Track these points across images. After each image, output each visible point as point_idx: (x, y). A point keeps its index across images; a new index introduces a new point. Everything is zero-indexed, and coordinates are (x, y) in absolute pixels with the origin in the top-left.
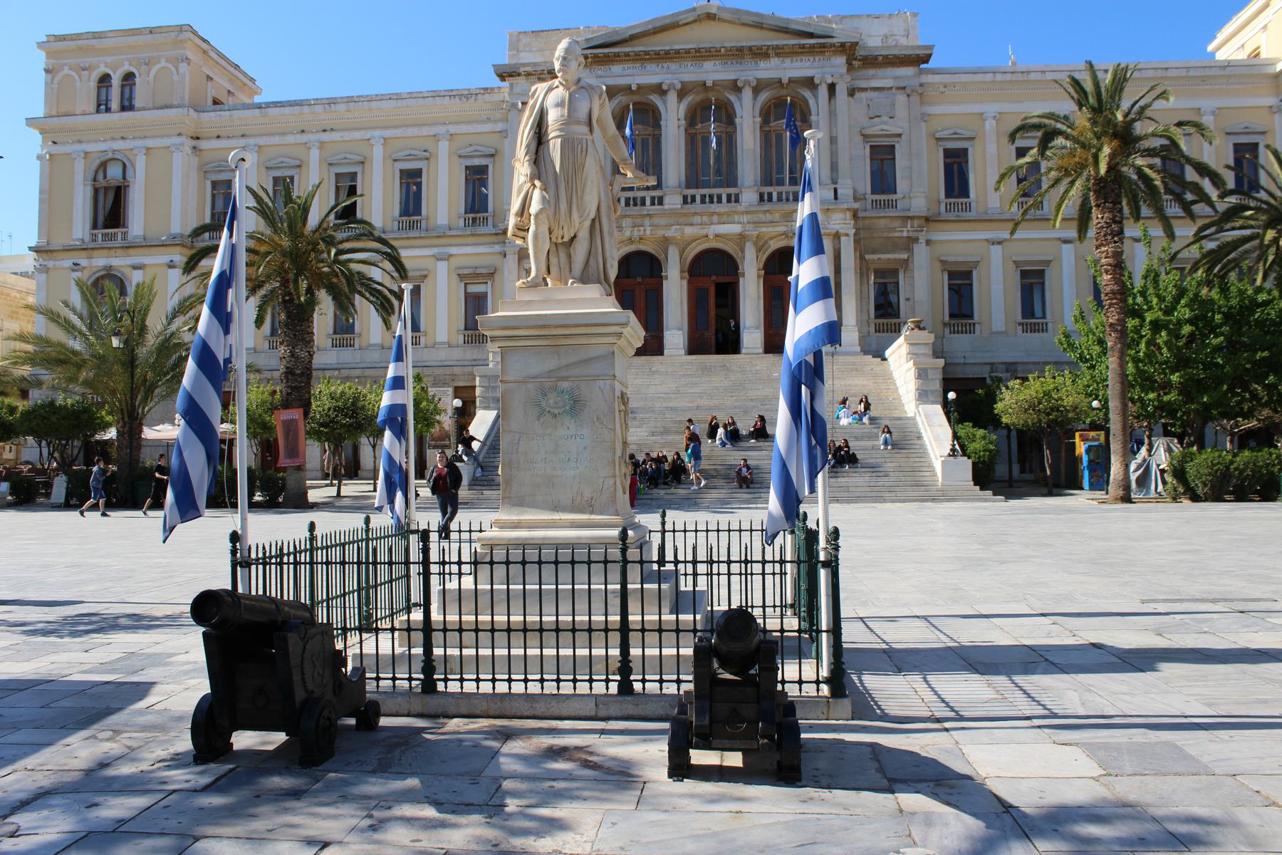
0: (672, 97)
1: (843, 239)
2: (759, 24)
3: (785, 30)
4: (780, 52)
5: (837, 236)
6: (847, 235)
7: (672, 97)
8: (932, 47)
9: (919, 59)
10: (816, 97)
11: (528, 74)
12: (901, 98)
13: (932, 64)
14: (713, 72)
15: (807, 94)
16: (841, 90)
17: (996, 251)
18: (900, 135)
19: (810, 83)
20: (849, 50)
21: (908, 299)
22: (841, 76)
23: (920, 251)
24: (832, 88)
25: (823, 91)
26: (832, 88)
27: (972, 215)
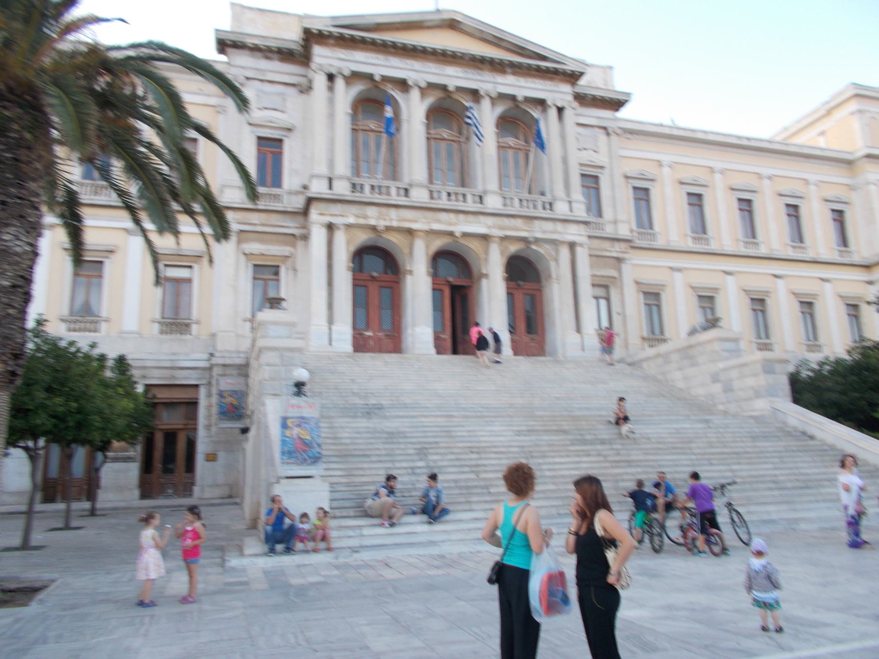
0: (415, 94)
1: (579, 250)
2: (497, 40)
3: (521, 50)
4: (517, 69)
5: (572, 246)
6: (581, 245)
7: (415, 94)
8: (628, 94)
9: (616, 104)
10: (546, 119)
11: (255, 49)
12: (601, 136)
13: (624, 113)
14: (454, 77)
15: (536, 113)
16: (568, 114)
17: (678, 276)
18: (602, 167)
19: (541, 103)
20: (573, 77)
21: (619, 314)
22: (569, 102)
23: (626, 268)
24: (560, 110)
25: (553, 113)
26: (560, 110)
27: (660, 243)
